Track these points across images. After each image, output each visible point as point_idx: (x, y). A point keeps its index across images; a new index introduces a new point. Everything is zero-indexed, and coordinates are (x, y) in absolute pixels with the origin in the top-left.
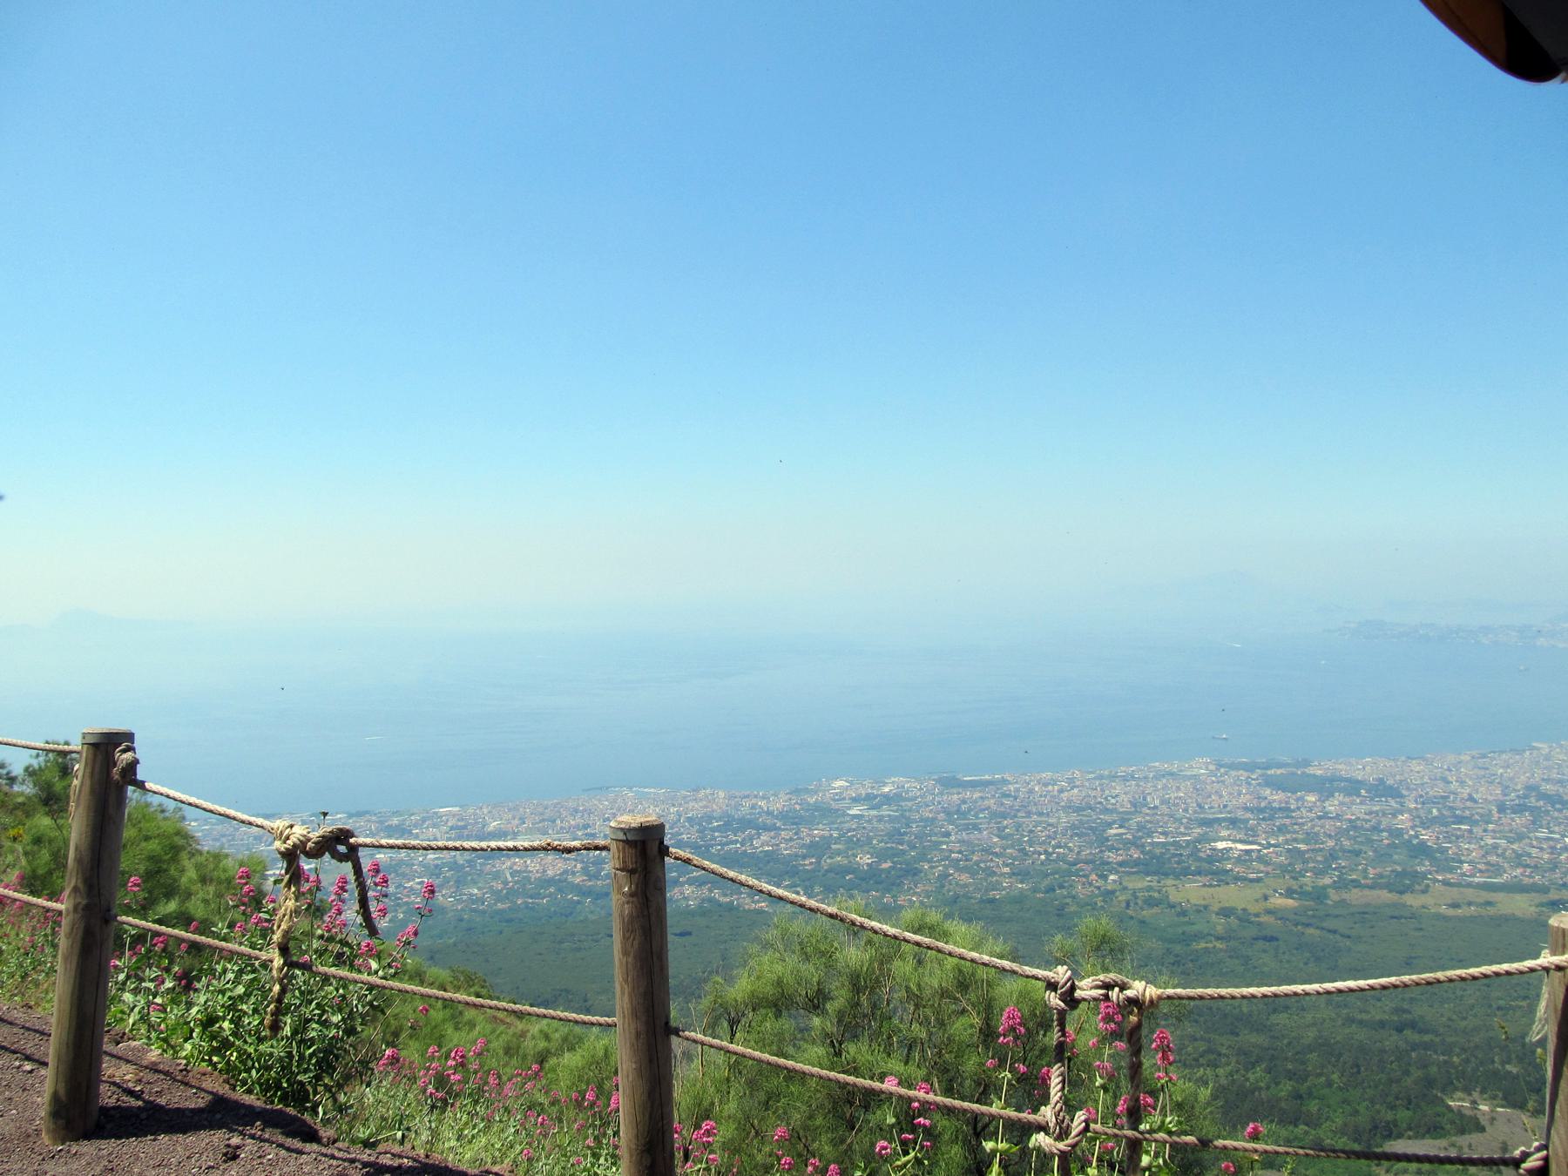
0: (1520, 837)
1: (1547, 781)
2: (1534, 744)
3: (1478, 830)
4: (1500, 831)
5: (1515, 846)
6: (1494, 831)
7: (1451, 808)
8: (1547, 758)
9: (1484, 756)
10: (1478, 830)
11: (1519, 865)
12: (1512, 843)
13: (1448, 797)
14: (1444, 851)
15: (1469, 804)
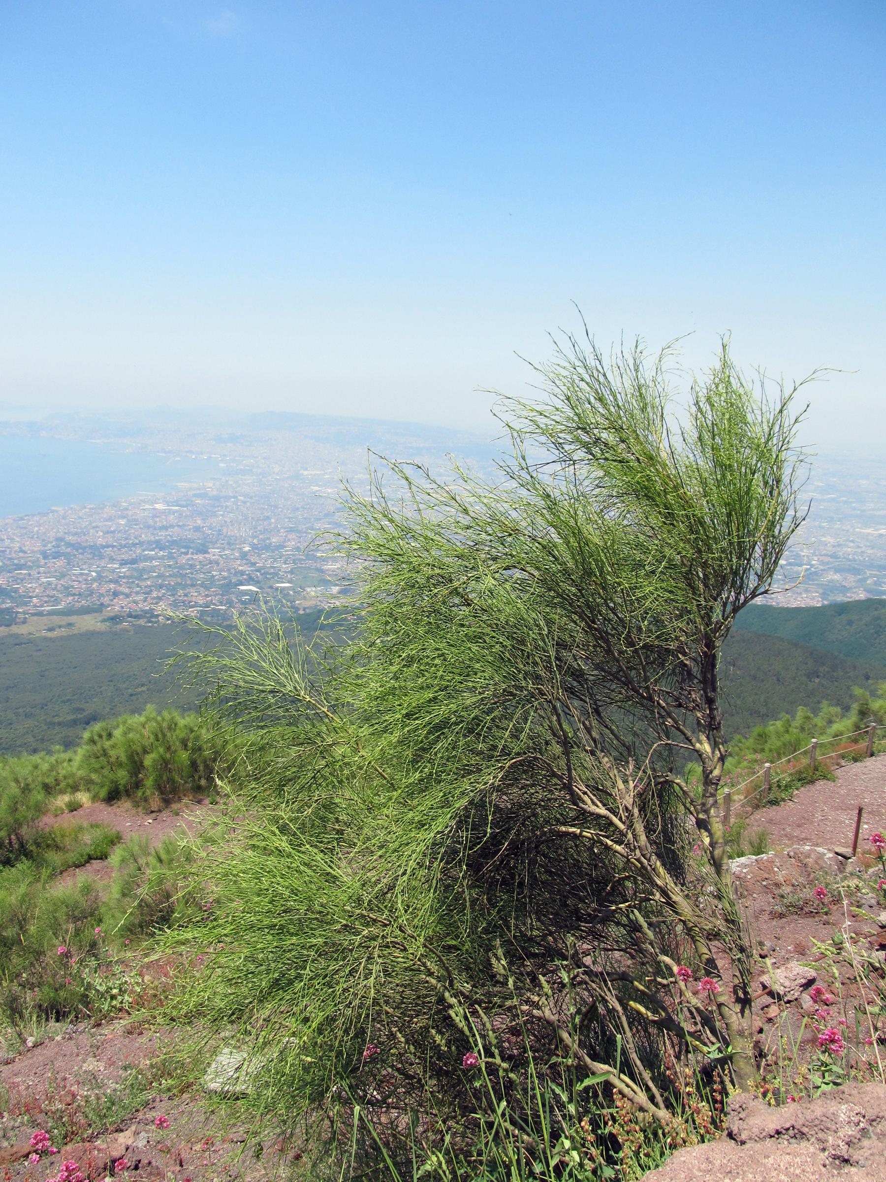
0: (63, 575)
1: (68, 533)
2: (54, 508)
3: (34, 573)
4: (49, 572)
5: (62, 582)
6: (45, 573)
7: (10, 559)
8: (64, 517)
9: (22, 519)
10: (34, 573)
11: (69, 595)
12: (59, 580)
13: (5, 551)
14: (16, 591)
15: (21, 554)
